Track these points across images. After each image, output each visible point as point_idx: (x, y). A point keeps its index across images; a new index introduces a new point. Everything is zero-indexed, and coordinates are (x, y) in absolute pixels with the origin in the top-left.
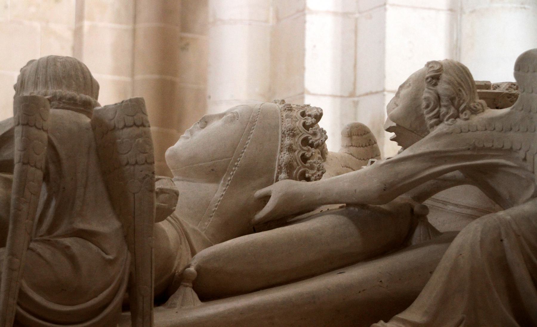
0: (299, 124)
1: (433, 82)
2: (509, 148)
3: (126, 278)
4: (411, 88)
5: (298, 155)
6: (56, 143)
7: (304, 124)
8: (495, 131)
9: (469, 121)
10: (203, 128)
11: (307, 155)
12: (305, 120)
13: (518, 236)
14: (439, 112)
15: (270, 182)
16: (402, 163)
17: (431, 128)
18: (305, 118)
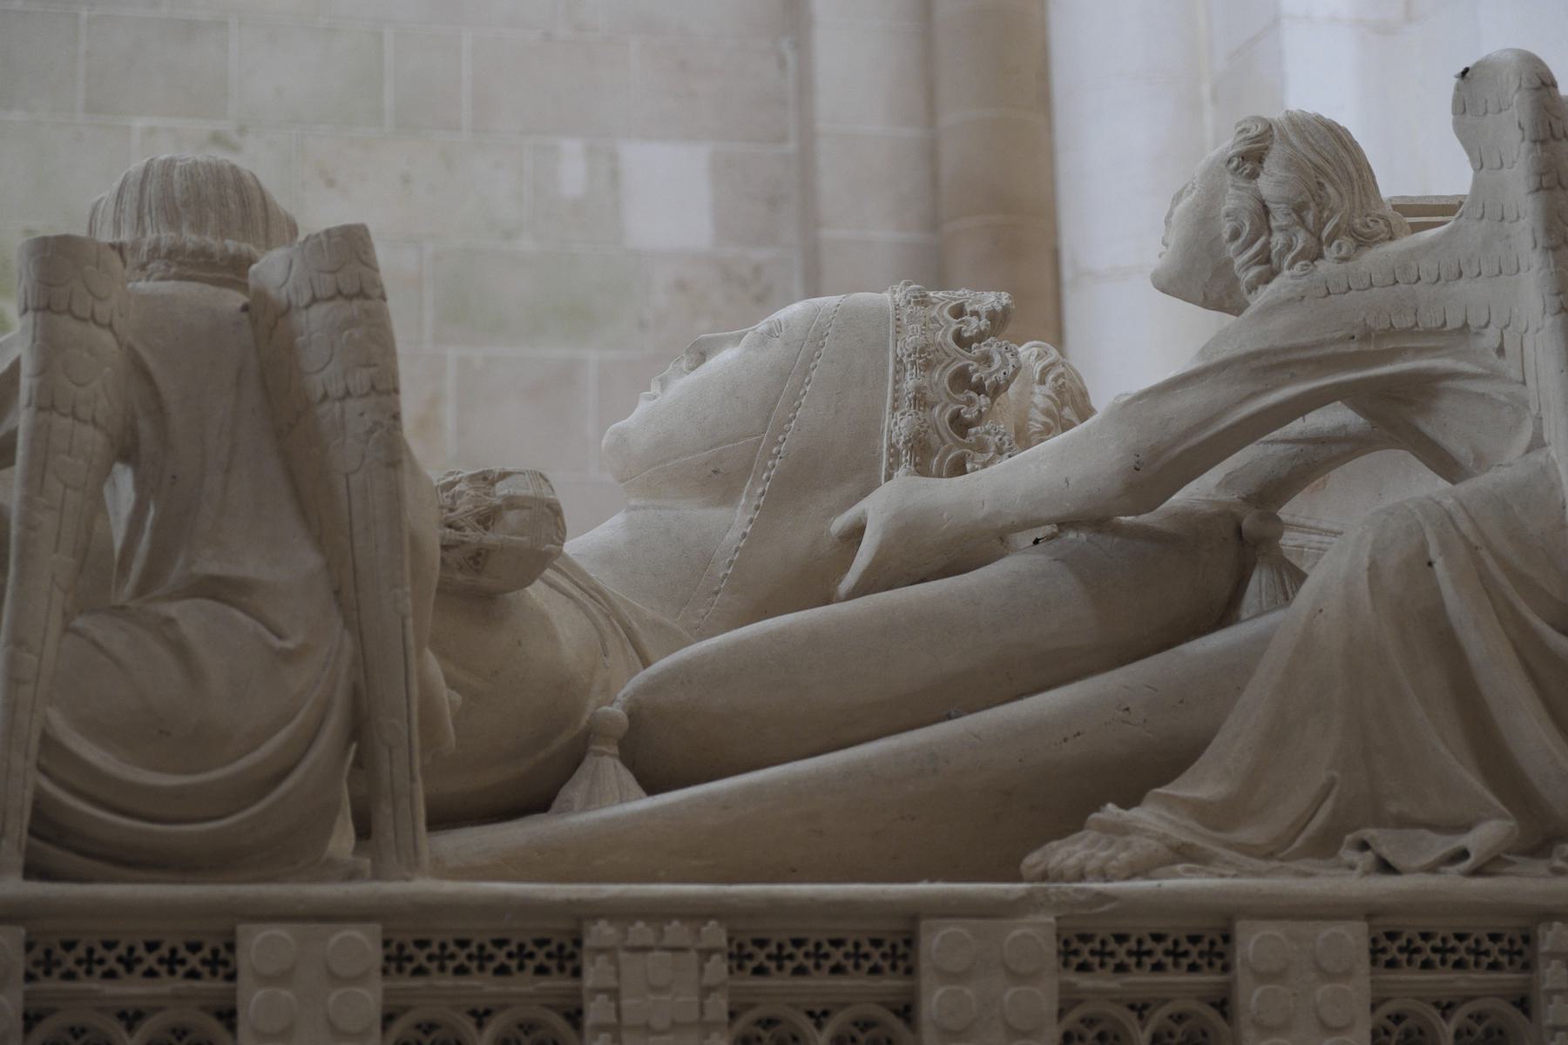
0: (944, 337)
1: (1245, 169)
2: (1460, 324)
3: (340, 700)
4: (1195, 192)
5: (941, 416)
6: (152, 363)
7: (959, 338)
8: (1419, 283)
9: (1349, 264)
10: (693, 369)
11: (965, 413)
12: (960, 326)
13: (1473, 549)
14: (1267, 245)
15: (865, 493)
17: (1250, 292)
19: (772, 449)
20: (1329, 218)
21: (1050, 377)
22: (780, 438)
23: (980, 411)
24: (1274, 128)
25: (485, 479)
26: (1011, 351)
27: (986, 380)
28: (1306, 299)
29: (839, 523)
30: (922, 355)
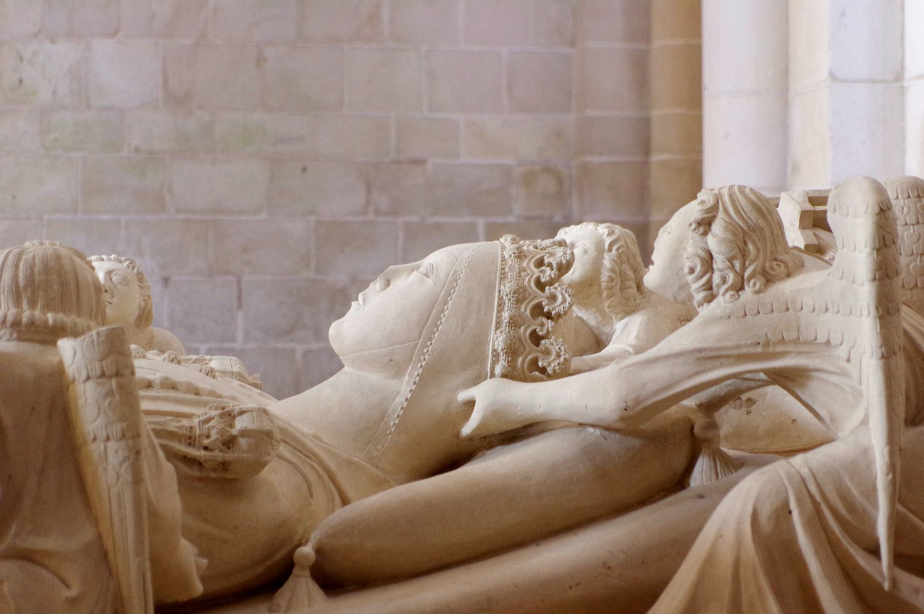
1: (700, 230)
2: (824, 340)
5: (524, 332)
9: (761, 295)
12: (539, 274)
14: (710, 279)
15: (478, 380)
16: (652, 366)
17: (699, 306)
18: (540, 270)
19: (423, 350)
20: (749, 265)
21: (615, 248)
22: (429, 343)
23: (548, 330)
24: (720, 203)
25: (230, 415)
26: (568, 293)
27: (552, 311)
28: (732, 318)
30: (515, 295)
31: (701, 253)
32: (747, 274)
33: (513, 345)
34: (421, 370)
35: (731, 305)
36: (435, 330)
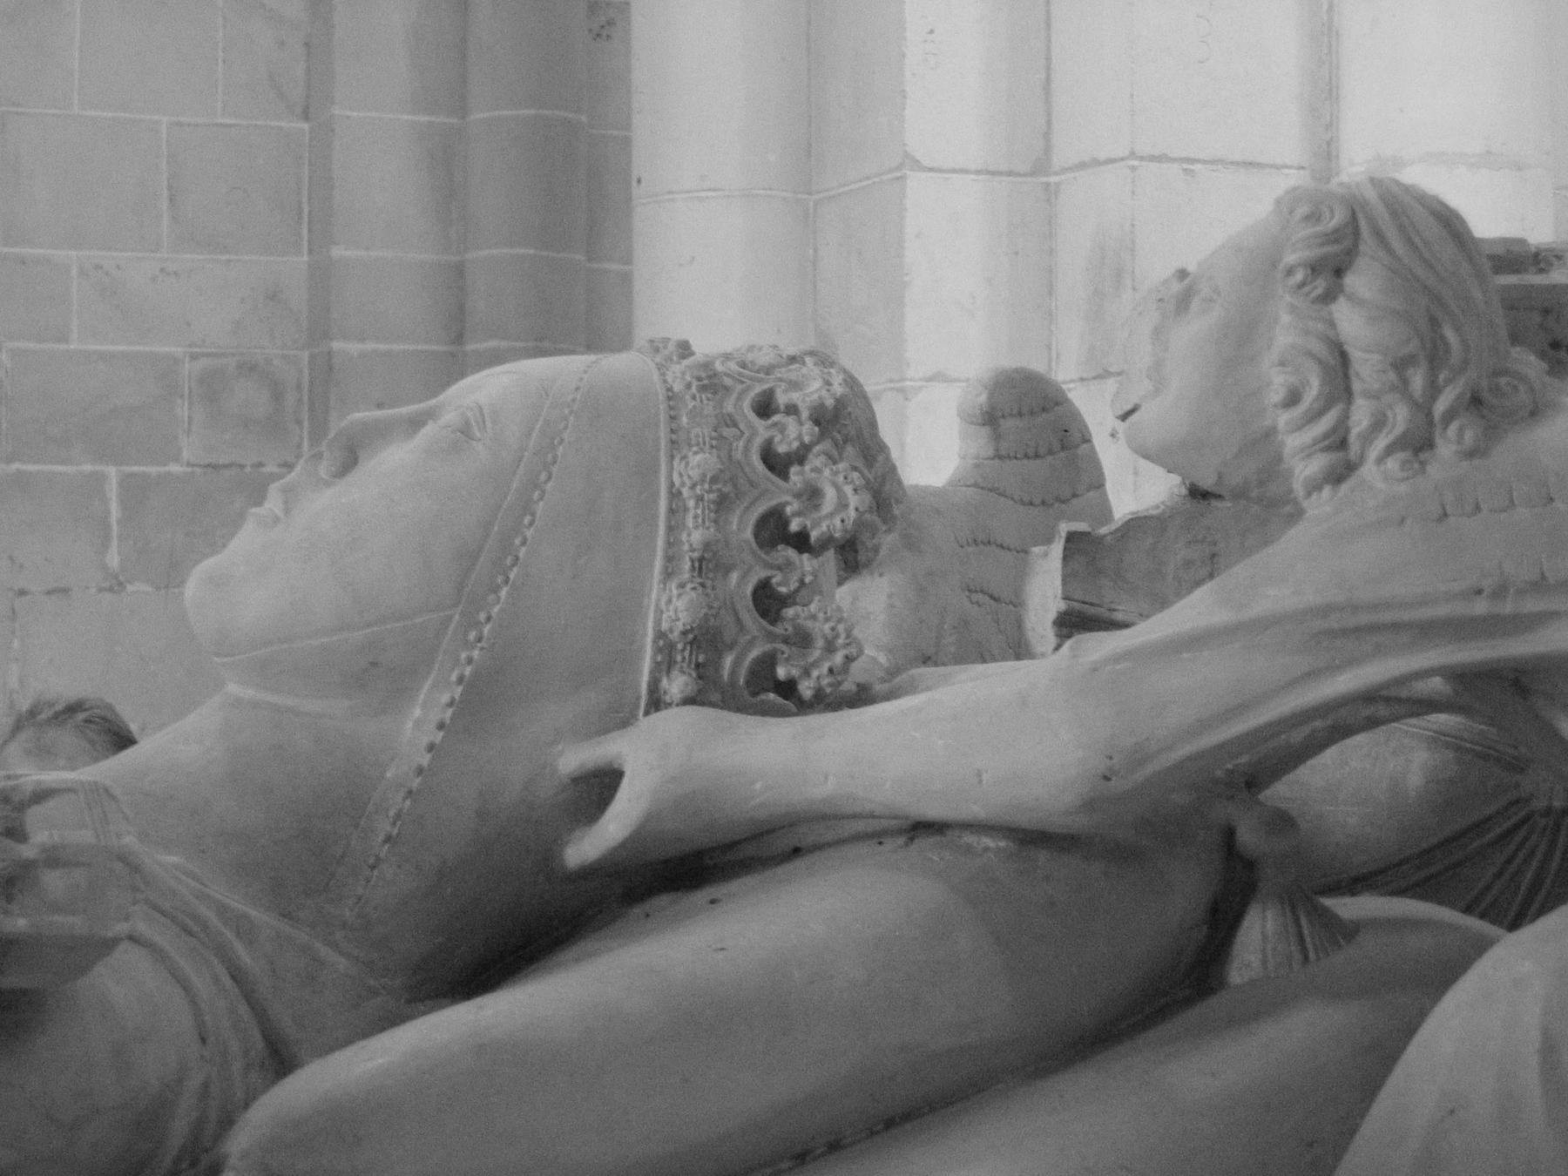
1: (1316, 288)
5: (740, 584)
11: (779, 584)
14: (1344, 419)
15: (619, 718)
16: (1185, 655)
17: (1309, 494)
18: (770, 422)
19: (466, 634)
20: (1448, 382)
22: (482, 616)
23: (802, 582)
24: (1360, 216)
27: (813, 528)
28: (1408, 522)
29: (574, 758)
30: (714, 487)
31: (1319, 348)
32: (1440, 406)
33: (712, 619)
34: (460, 689)
35: (1403, 488)
36: (500, 579)
